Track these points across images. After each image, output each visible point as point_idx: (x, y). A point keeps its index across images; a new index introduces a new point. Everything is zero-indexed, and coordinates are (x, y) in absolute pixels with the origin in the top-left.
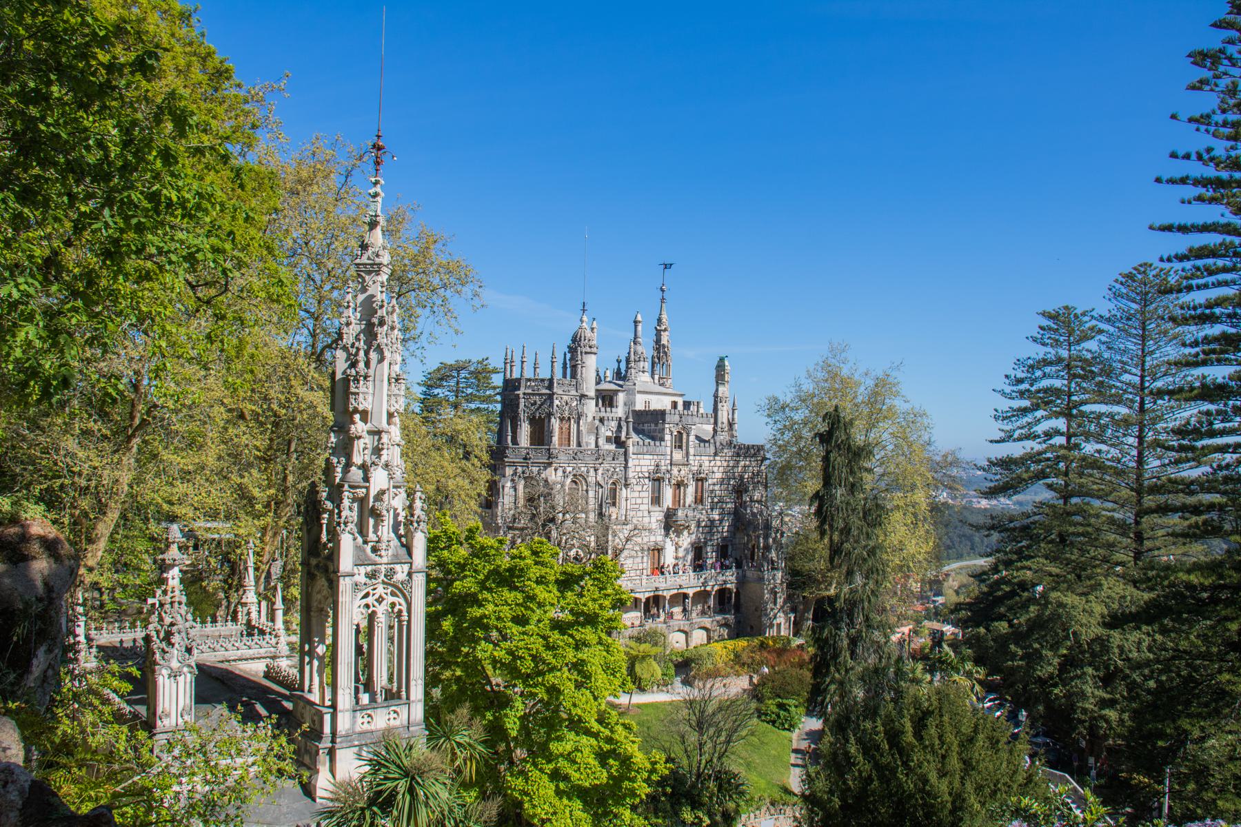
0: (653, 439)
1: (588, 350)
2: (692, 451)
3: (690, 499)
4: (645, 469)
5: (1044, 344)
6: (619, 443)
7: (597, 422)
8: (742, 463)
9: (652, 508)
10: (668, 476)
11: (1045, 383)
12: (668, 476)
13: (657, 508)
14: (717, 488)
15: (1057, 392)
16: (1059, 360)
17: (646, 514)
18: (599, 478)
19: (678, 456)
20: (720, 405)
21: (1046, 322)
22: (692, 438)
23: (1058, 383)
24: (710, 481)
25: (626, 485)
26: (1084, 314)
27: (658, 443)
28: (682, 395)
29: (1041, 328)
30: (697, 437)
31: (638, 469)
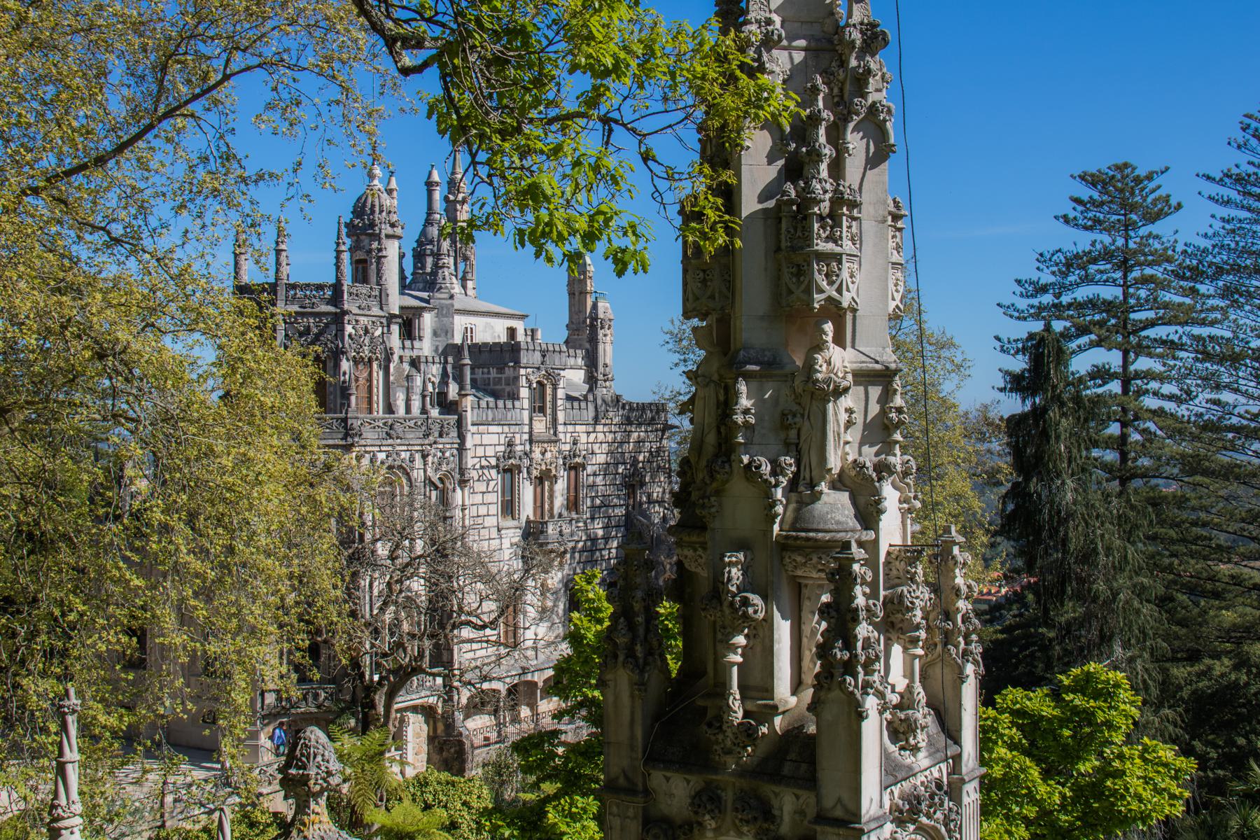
0: (496, 395)
1: (390, 231)
2: (561, 417)
3: (559, 501)
4: (490, 451)
5: (1086, 228)
6: (448, 406)
7: (406, 367)
9: (503, 524)
10: (526, 462)
11: (1083, 293)
12: (526, 462)
13: (510, 523)
14: (599, 480)
15: (1108, 306)
16: (1107, 255)
17: (494, 533)
18: (430, 472)
19: (540, 426)
20: (601, 332)
21: (1086, 193)
22: (561, 393)
23: (1110, 293)
24: (590, 469)
25: (463, 483)
26: (1149, 178)
28: (523, 317)
29: (1078, 201)
30: (569, 398)
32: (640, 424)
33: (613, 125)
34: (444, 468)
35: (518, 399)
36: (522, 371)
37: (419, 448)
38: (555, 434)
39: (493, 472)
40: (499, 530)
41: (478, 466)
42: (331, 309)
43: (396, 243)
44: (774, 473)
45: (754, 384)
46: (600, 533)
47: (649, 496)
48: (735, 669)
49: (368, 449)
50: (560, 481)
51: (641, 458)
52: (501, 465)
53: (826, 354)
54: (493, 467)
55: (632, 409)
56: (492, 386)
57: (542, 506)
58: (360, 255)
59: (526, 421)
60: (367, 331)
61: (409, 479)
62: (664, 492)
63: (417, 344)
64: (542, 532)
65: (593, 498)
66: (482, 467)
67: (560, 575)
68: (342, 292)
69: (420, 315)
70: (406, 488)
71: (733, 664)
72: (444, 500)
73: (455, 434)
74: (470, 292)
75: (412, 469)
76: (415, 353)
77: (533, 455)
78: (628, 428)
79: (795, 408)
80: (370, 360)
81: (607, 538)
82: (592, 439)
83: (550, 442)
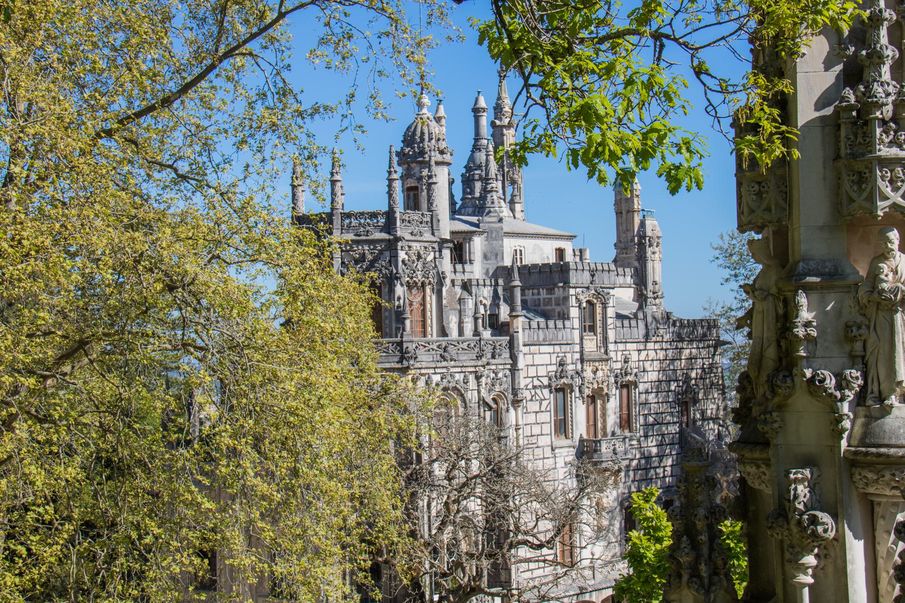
0: (546, 316)
1: (439, 158)
2: (611, 335)
3: (612, 419)
4: (542, 371)
6: (499, 328)
7: (458, 290)
8: (686, 352)
10: (578, 381)
12: (578, 381)
13: (564, 442)
17: (548, 453)
18: (484, 393)
19: (591, 344)
20: (649, 251)
22: (611, 312)
24: (642, 387)
25: (516, 403)
27: (560, 324)
28: (571, 238)
30: (619, 316)
31: (532, 372)
32: (691, 341)
33: (665, 40)
34: (497, 388)
35: (568, 318)
36: (572, 291)
37: (472, 369)
38: (606, 353)
39: (546, 391)
40: (553, 450)
41: (530, 386)
42: (384, 236)
43: (445, 169)
44: (839, 387)
45: (815, 296)
46: (654, 451)
47: (703, 413)
48: (806, 591)
49: (423, 371)
50: (612, 400)
51: (693, 375)
52: (554, 385)
53: (892, 263)
54: (545, 387)
55: (682, 326)
56: (542, 307)
57: (595, 425)
58: (411, 183)
59: (577, 340)
60: (419, 257)
61: (464, 401)
62: (718, 409)
63: (468, 267)
64: (596, 451)
65: (645, 416)
66: (534, 387)
67: (615, 493)
68: (395, 219)
69: (470, 239)
70: (461, 410)
71: (804, 585)
72: (498, 420)
73: (508, 355)
74: (518, 215)
75: (466, 390)
76: (466, 277)
77: (585, 374)
78: (680, 345)
79: (859, 319)
80: (423, 285)
81: (661, 456)
82: (642, 357)
83: (601, 360)
